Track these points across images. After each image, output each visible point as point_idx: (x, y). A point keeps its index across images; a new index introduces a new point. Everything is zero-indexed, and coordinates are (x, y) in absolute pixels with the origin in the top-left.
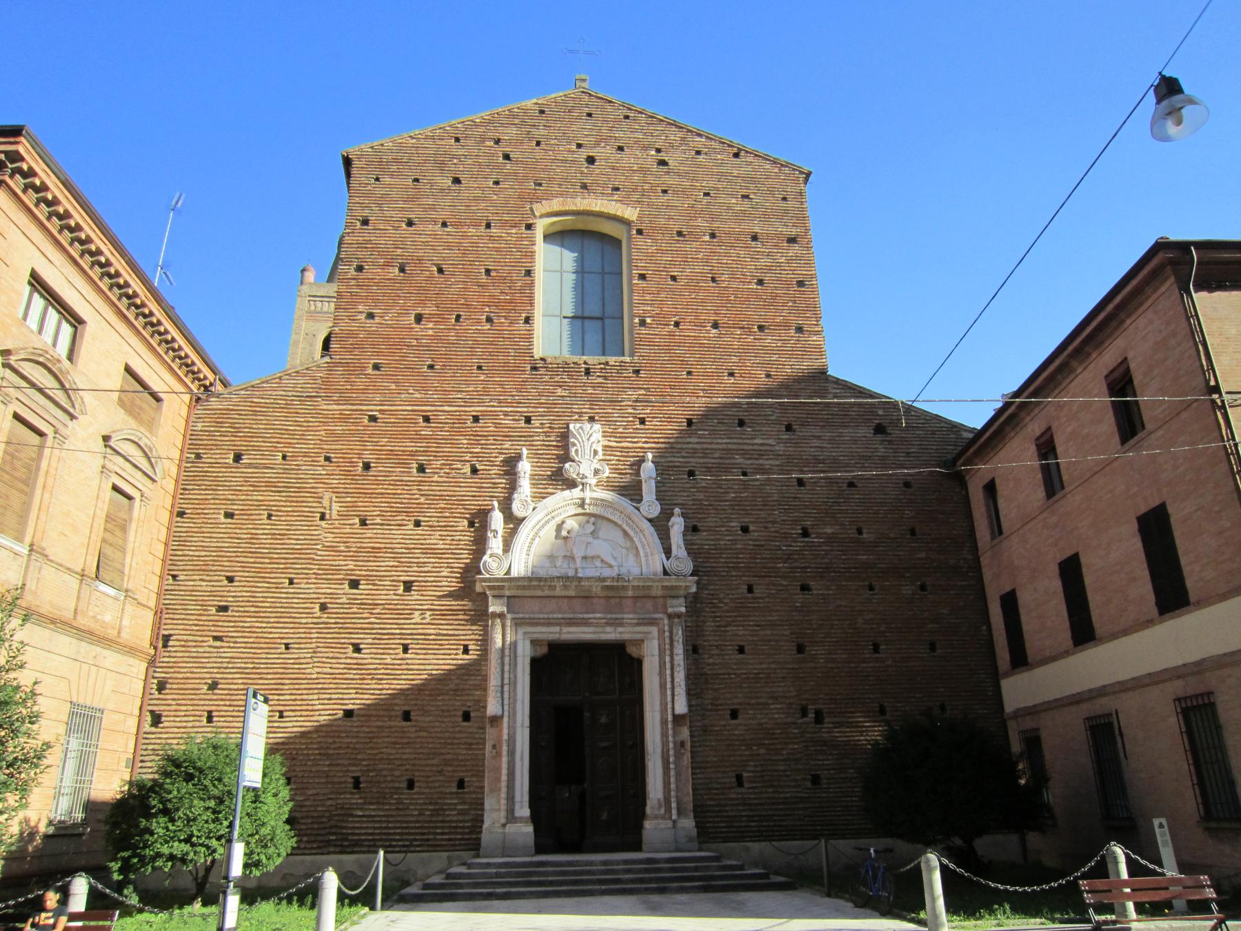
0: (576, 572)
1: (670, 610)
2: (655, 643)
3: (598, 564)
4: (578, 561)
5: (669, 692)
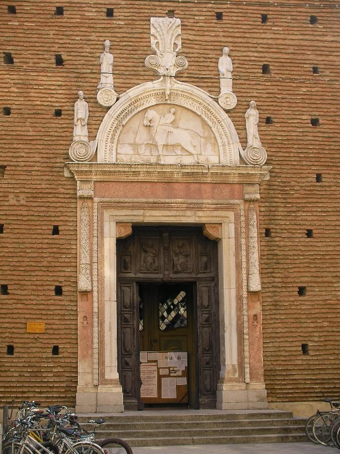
0: (158, 160)
1: (247, 196)
2: (232, 226)
3: (179, 152)
4: (160, 148)
5: (244, 271)
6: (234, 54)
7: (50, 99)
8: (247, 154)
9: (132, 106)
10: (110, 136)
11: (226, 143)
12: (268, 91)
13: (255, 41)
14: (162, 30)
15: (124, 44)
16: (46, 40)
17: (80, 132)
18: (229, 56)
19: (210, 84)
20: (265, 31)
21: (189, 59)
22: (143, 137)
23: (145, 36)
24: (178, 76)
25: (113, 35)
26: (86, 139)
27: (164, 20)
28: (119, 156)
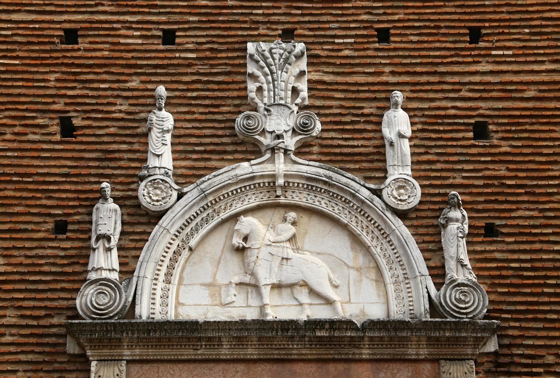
3: (304, 296)
4: (266, 291)
6: (415, 105)
7: (44, 202)
8: (450, 296)
9: (210, 211)
10: (164, 269)
11: (401, 278)
12: (488, 173)
13: (456, 79)
14: (269, 66)
15: (195, 94)
16: (41, 92)
17: (105, 262)
18: (405, 109)
19: (365, 165)
20: (476, 59)
21: (324, 119)
22: (232, 271)
23: (239, 78)
24: (302, 150)
25: (174, 79)
26: (115, 276)
27: (273, 45)
28: (181, 310)
